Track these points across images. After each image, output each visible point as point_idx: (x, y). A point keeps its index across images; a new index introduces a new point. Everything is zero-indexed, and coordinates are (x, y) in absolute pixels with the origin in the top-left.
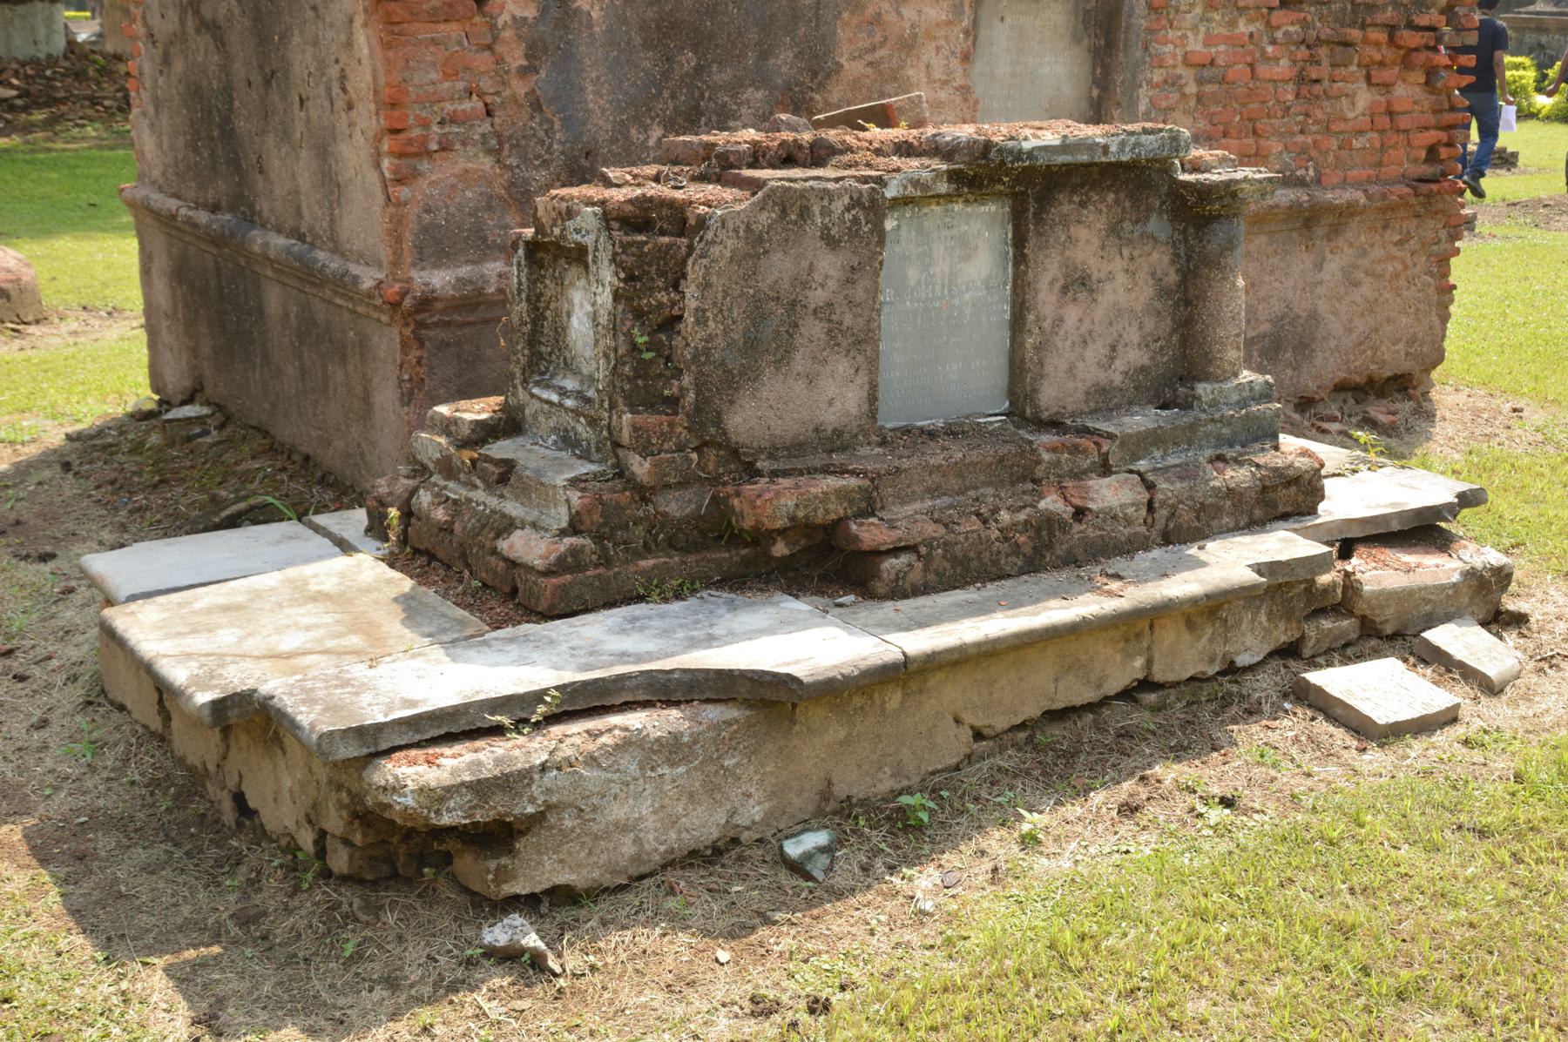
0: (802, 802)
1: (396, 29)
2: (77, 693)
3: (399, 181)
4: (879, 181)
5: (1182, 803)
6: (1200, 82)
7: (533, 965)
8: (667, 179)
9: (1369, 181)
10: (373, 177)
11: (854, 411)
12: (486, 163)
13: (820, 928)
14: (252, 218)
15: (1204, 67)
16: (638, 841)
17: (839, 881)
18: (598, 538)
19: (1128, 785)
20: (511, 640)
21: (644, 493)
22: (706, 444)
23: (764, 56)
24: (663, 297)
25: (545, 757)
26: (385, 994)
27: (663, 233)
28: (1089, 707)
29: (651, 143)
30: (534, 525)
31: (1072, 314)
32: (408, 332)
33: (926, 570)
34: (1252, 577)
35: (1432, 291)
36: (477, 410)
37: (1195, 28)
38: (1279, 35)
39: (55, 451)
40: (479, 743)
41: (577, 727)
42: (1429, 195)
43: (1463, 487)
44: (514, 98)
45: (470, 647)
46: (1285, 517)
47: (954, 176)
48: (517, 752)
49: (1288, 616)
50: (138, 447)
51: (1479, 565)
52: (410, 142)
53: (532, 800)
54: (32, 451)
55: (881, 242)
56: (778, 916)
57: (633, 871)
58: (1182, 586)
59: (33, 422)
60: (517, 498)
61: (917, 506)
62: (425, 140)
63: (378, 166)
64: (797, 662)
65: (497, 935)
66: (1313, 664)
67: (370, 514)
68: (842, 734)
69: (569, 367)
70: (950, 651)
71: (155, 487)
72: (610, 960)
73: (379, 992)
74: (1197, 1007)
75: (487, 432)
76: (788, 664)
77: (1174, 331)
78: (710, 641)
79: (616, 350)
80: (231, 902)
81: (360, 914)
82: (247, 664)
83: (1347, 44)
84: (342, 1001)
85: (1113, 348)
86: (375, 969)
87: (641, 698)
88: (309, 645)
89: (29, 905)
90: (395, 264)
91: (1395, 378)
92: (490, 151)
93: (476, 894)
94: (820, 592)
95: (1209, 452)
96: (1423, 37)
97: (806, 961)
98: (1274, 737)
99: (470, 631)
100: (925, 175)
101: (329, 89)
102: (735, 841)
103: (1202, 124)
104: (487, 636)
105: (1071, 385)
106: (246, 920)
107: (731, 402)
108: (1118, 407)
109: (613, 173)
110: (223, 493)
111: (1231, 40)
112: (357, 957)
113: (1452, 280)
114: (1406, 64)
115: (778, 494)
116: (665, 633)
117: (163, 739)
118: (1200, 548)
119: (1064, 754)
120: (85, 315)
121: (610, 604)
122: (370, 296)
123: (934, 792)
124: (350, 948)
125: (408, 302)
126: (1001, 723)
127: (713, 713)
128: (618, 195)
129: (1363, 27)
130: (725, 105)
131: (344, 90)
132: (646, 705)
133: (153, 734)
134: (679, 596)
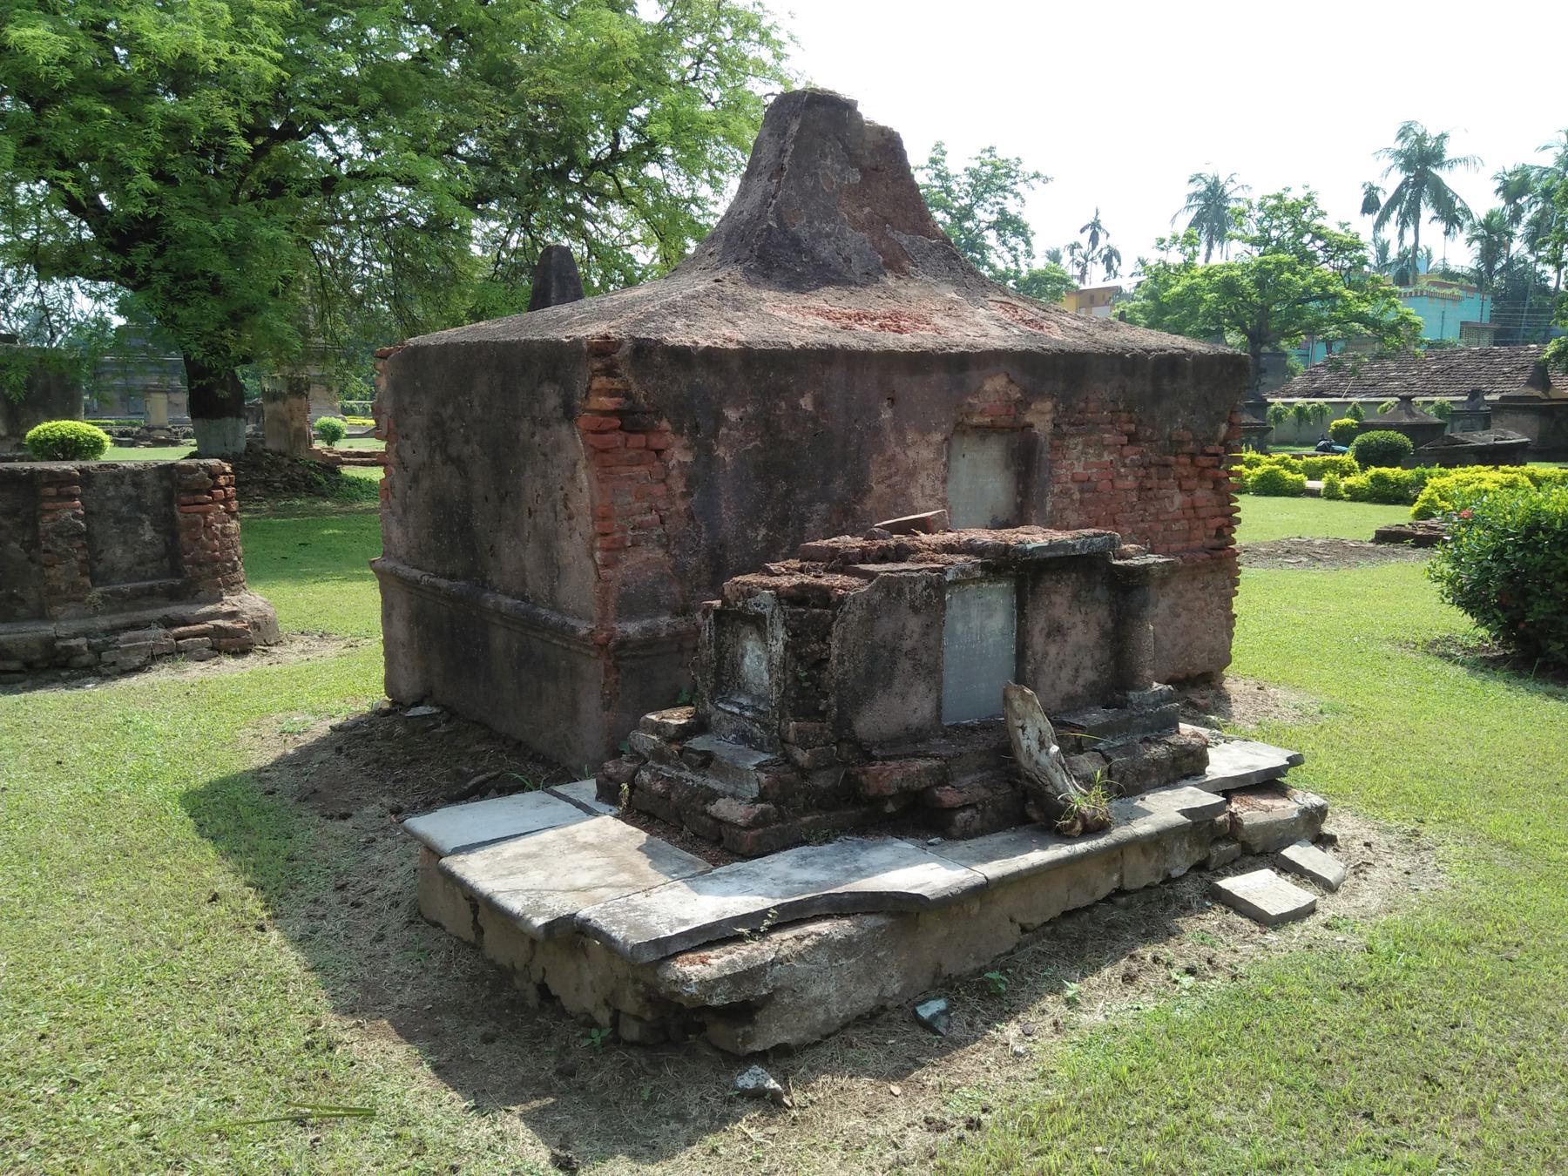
0: (922, 981)
1: (607, 470)
2: (402, 914)
3: (606, 566)
4: (941, 570)
5: (1162, 972)
6: (1082, 491)
7: (773, 1103)
8: (808, 571)
9: (1183, 550)
10: (589, 563)
11: (928, 716)
12: (660, 553)
13: (953, 1068)
14: (484, 584)
15: (1085, 484)
16: (827, 1011)
17: (956, 1034)
18: (777, 805)
19: (1124, 961)
20: (731, 874)
21: (804, 773)
22: (841, 740)
23: (827, 482)
24: (815, 647)
25: (773, 956)
26: (678, 1126)
27: (815, 606)
28: (1087, 908)
29: (759, 538)
30: (734, 796)
31: (1053, 650)
32: (610, 663)
33: (982, 819)
34: (1182, 819)
35: (1222, 618)
36: (677, 718)
37: (1078, 459)
38: (1127, 461)
39: (325, 739)
40: (729, 948)
41: (788, 934)
42: (1220, 558)
43: (1290, 754)
44: (678, 512)
45: (705, 880)
46: (1187, 777)
47: (984, 566)
48: (756, 953)
49: (1200, 842)
50: (388, 736)
51: (1309, 806)
52: (614, 541)
53: (766, 986)
54: (307, 739)
55: (944, 609)
56: (922, 1060)
57: (824, 1032)
58: (1142, 827)
59: (302, 718)
60: (717, 777)
61: (973, 777)
62: (624, 539)
63: (592, 556)
64: (921, 885)
65: (747, 1081)
66: (1222, 877)
67: (599, 785)
68: (945, 933)
69: (742, 689)
70: (1012, 875)
71: (409, 764)
72: (821, 1095)
73: (674, 1125)
74: (1217, 1116)
75: (685, 732)
76: (916, 887)
77: (1111, 658)
78: (859, 872)
79: (785, 681)
80: (549, 1067)
81: (648, 1070)
82: (560, 896)
83: (1167, 466)
84: (650, 1133)
85: (1077, 671)
86: (667, 1108)
87: (824, 912)
88: (596, 881)
89: (412, 1070)
90: (603, 619)
91: (1203, 675)
92: (663, 546)
93: (722, 1051)
94: (917, 837)
95: (1139, 737)
97: (953, 1092)
98: (1205, 925)
99: (701, 869)
100: (968, 566)
101: (554, 506)
102: (883, 1008)
103: (1084, 518)
104: (714, 872)
105: (1053, 695)
106: (566, 1073)
107: (858, 713)
108: (1081, 708)
109: (773, 567)
110: (466, 769)
111: (1099, 466)
112: (652, 1101)
113: (1234, 611)
114: (1201, 476)
115: (891, 772)
116: (828, 867)
117: (476, 947)
118: (1143, 799)
119: (1077, 941)
120: (306, 639)
121: (785, 848)
122: (584, 639)
123: (1003, 970)
124: (646, 1095)
125: (612, 644)
126: (1037, 921)
127: (870, 921)
128: (785, 582)
129: (1176, 455)
130: (803, 514)
131: (566, 507)
132: (827, 917)
133: (467, 944)
134: (828, 841)
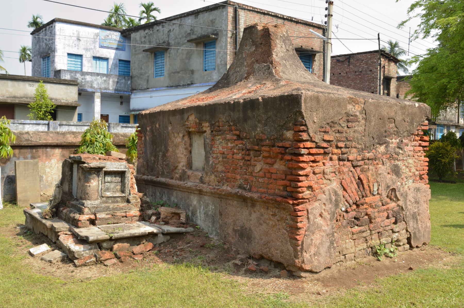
6: (223, 158)
96: (279, 150)
111: (227, 148)
